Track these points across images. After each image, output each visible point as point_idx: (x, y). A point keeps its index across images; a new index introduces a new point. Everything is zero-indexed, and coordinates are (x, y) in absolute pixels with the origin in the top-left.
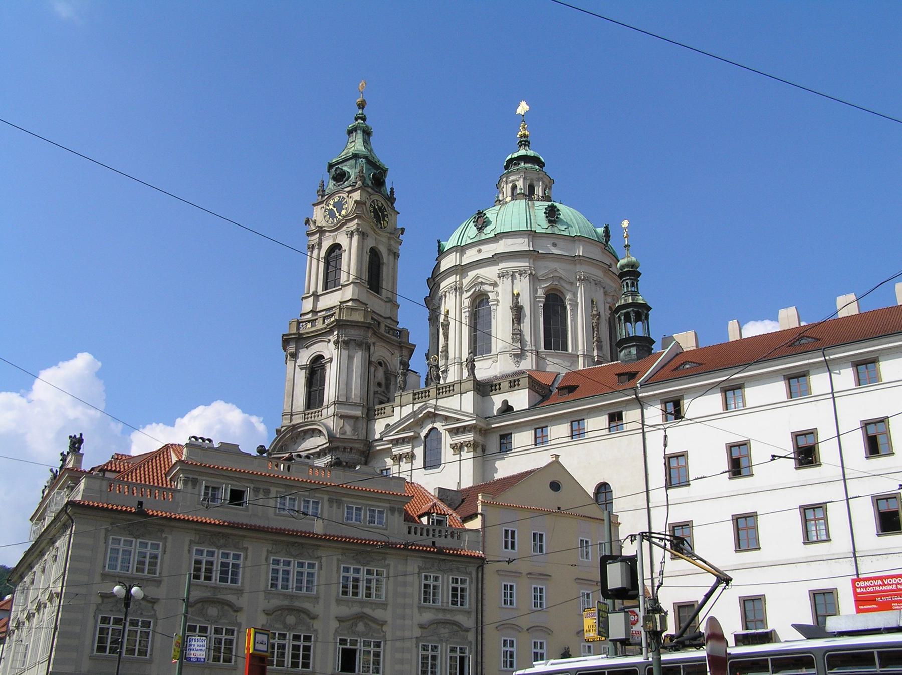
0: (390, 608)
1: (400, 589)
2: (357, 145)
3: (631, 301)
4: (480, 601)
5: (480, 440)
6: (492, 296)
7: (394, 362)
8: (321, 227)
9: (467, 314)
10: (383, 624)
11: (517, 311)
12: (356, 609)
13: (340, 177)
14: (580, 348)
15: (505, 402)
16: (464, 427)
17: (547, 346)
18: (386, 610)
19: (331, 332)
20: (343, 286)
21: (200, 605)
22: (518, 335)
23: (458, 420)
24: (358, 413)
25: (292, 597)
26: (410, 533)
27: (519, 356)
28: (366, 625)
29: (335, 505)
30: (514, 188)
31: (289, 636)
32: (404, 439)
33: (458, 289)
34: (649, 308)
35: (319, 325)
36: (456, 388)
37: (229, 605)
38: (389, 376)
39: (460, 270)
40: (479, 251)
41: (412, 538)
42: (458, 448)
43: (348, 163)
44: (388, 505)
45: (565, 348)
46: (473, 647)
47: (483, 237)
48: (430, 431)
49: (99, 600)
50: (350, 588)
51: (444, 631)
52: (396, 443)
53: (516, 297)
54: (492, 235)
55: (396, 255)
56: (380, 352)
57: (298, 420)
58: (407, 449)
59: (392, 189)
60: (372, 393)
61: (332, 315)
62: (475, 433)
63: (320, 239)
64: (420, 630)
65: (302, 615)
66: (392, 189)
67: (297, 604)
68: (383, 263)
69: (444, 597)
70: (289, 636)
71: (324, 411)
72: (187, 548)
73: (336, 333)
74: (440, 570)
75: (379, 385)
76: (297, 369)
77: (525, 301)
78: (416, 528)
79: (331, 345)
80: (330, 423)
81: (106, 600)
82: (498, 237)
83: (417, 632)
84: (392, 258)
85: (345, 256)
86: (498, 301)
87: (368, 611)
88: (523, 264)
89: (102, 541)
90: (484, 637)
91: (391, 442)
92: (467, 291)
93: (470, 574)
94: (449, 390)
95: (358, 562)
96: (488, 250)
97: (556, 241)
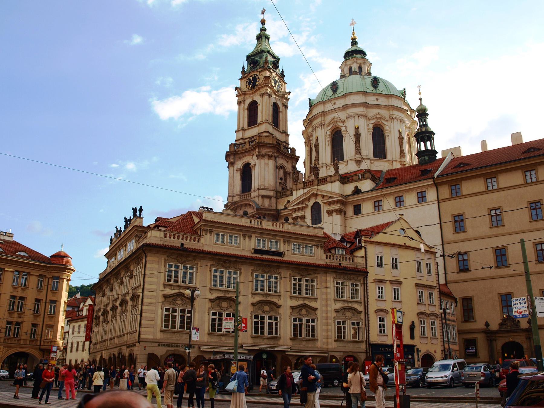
0: (319, 300)
1: (324, 290)
3: (424, 130)
4: (366, 296)
5: (343, 208)
6: (343, 129)
7: (289, 167)
8: (245, 92)
9: (329, 139)
10: (316, 309)
11: (357, 136)
12: (301, 302)
15: (356, 187)
16: (334, 201)
18: (316, 302)
19: (254, 149)
21: (218, 301)
22: (358, 150)
23: (330, 197)
24: (271, 193)
25: (266, 295)
26: (327, 258)
27: (359, 162)
28: (307, 310)
29: (287, 244)
30: (351, 69)
31: (266, 318)
32: (299, 208)
34: (434, 134)
35: (247, 146)
36: (329, 179)
38: (286, 173)
39: (324, 114)
40: (335, 104)
41: (330, 262)
42: (330, 213)
43: (258, 56)
44: (315, 243)
46: (364, 322)
47: (337, 95)
48: (314, 203)
49: (163, 299)
50: (297, 289)
51: (348, 314)
52: (295, 210)
53: (357, 129)
54: (342, 94)
55: (286, 107)
56: (281, 161)
57: (236, 199)
58: (300, 214)
59: (283, 70)
60: (278, 184)
61: (254, 140)
62: (341, 204)
63: (244, 98)
65: (272, 306)
66: (283, 70)
67: (269, 299)
68: (280, 112)
69: (347, 294)
70: (266, 318)
71: (252, 194)
73: (257, 150)
74: (344, 279)
75: (281, 179)
76: (235, 171)
78: (330, 256)
79: (255, 157)
80: (256, 200)
82: (345, 95)
83: (334, 314)
84: (284, 108)
87: (307, 302)
88: (361, 110)
89: (163, 266)
90: (369, 316)
91: (291, 210)
93: (360, 281)
94: (324, 181)
95: (301, 275)
96: (340, 103)
97: (378, 97)
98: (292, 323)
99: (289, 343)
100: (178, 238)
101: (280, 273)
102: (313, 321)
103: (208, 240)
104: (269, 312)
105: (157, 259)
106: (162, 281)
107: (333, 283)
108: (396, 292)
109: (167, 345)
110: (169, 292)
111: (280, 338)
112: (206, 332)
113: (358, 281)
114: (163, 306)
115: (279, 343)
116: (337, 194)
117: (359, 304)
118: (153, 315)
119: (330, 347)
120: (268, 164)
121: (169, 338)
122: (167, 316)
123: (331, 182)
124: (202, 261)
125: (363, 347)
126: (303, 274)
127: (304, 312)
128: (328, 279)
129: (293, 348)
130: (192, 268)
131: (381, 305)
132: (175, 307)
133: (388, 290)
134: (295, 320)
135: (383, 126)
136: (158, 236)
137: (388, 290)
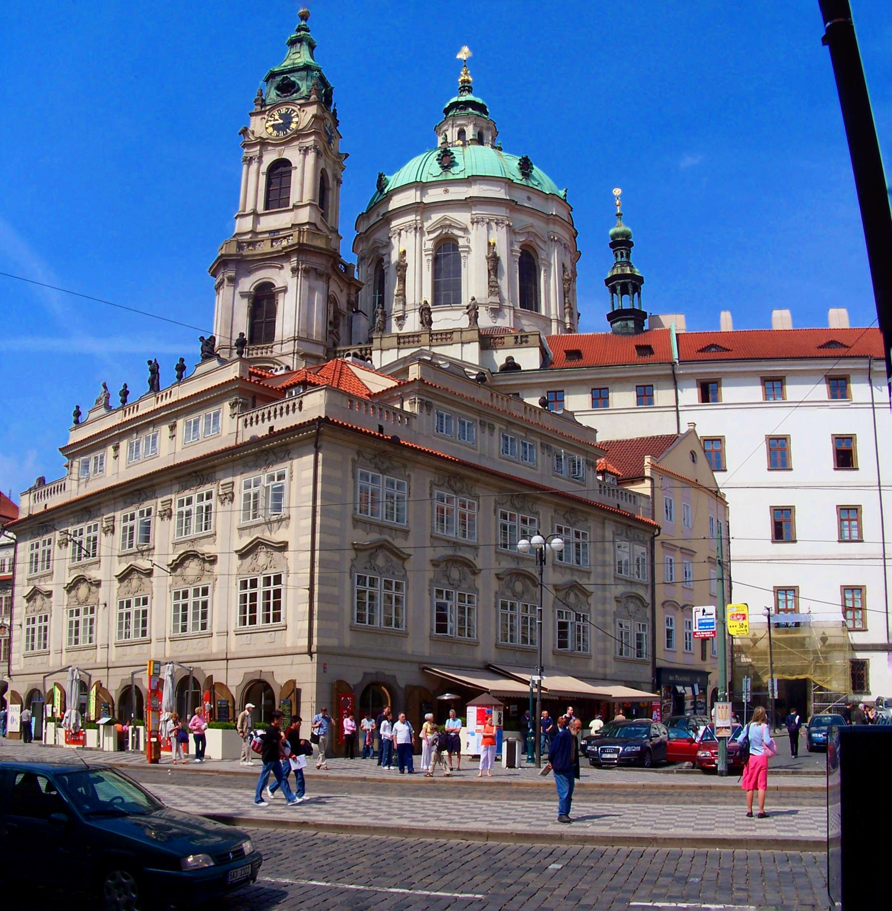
2: (302, 57)
6: (461, 242)
11: (494, 261)
13: (287, 88)
14: (553, 312)
15: (510, 359)
17: (523, 305)
20: (296, 207)
33: (419, 230)
43: (296, 74)
45: (537, 309)
47: (450, 177)
54: (461, 176)
66: (335, 110)
77: (502, 252)
82: (471, 180)
85: (296, 176)
86: (468, 247)
88: (501, 212)
92: (429, 233)
135: (538, 249)
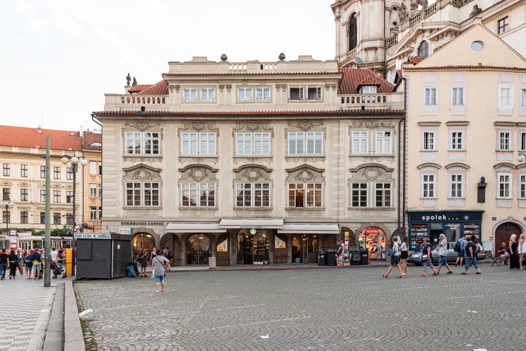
0: (327, 159)
12: (301, 163)
15: (476, 7)
16: (442, 34)
18: (324, 161)
21: (189, 170)
23: (438, 29)
28: (309, 173)
31: (253, 185)
36: (438, 6)
37: (209, 168)
49: (124, 174)
51: (372, 174)
64: (351, 173)
65: (261, 170)
67: (256, 163)
70: (253, 185)
72: (176, 134)
81: (128, 173)
83: (350, 175)
87: (310, 163)
93: (394, 127)
98: (289, 189)
99: (285, 214)
100: (139, 102)
101: (271, 129)
102: (319, 186)
103: (175, 98)
104: (256, 179)
105: (114, 129)
106: (121, 154)
107: (349, 134)
108: (457, 138)
109: (131, 224)
110: (129, 164)
111: (271, 210)
112: (177, 206)
113: (390, 127)
114: (124, 181)
115: (270, 215)
116: (444, 23)
117: (390, 159)
118: (114, 192)
119: (341, 217)
120: (373, 7)
121: (133, 215)
122: (129, 192)
123: (441, 8)
124: (167, 125)
125: (394, 215)
126: (304, 126)
127: (305, 175)
128: (342, 129)
129: (286, 221)
130: (156, 135)
131: (429, 158)
132: (137, 181)
133: (443, 137)
134: (292, 186)
136: (113, 102)
137: (443, 137)
